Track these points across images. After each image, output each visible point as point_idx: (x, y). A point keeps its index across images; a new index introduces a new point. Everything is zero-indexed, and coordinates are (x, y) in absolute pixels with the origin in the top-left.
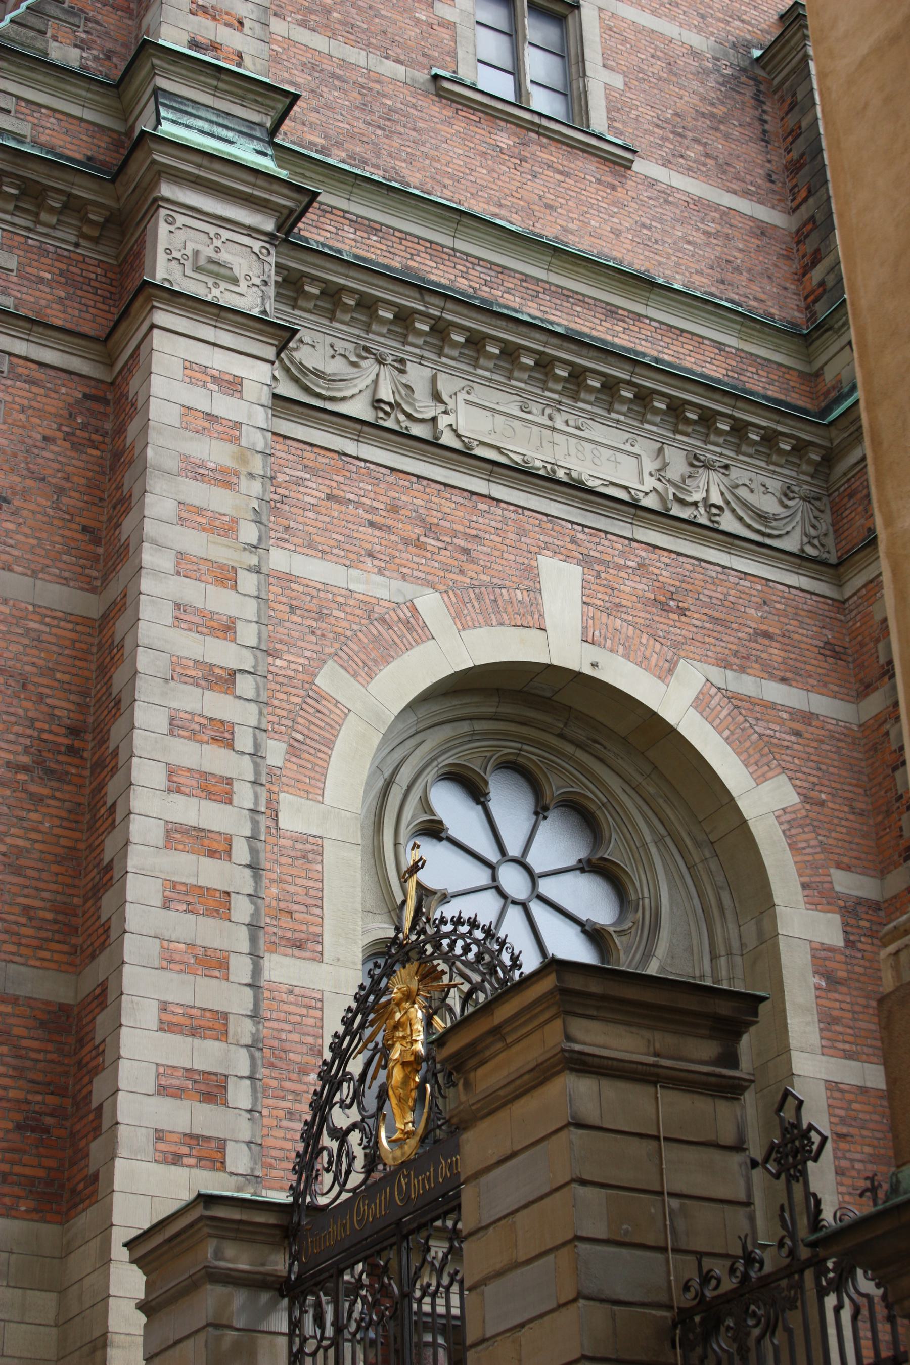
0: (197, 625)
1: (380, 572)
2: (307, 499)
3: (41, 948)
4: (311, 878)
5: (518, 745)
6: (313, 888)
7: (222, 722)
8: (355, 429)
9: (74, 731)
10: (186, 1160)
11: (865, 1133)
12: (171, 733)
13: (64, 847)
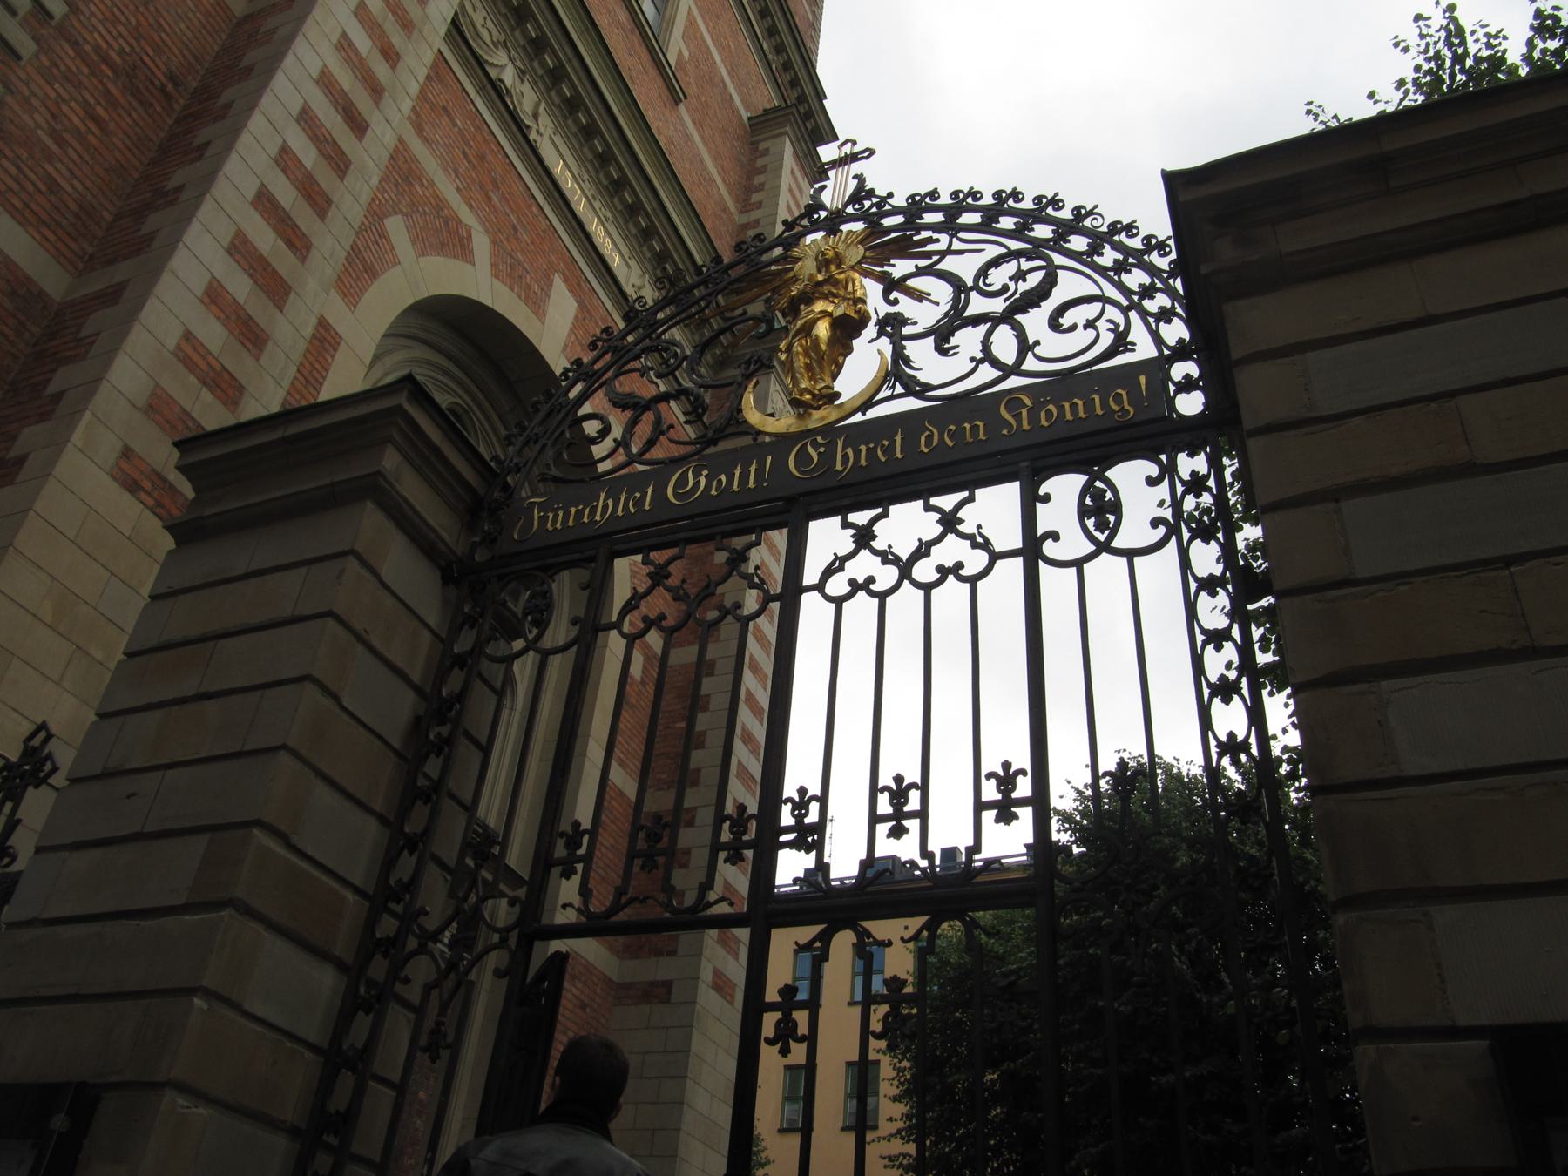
0: (354, 65)
1: (458, 189)
2: (429, 94)
3: (48, 227)
4: (320, 363)
5: (471, 403)
6: (318, 372)
7: (343, 152)
8: (482, 83)
9: (172, 78)
10: (143, 496)
11: (614, 827)
12: (298, 121)
13: (117, 161)
